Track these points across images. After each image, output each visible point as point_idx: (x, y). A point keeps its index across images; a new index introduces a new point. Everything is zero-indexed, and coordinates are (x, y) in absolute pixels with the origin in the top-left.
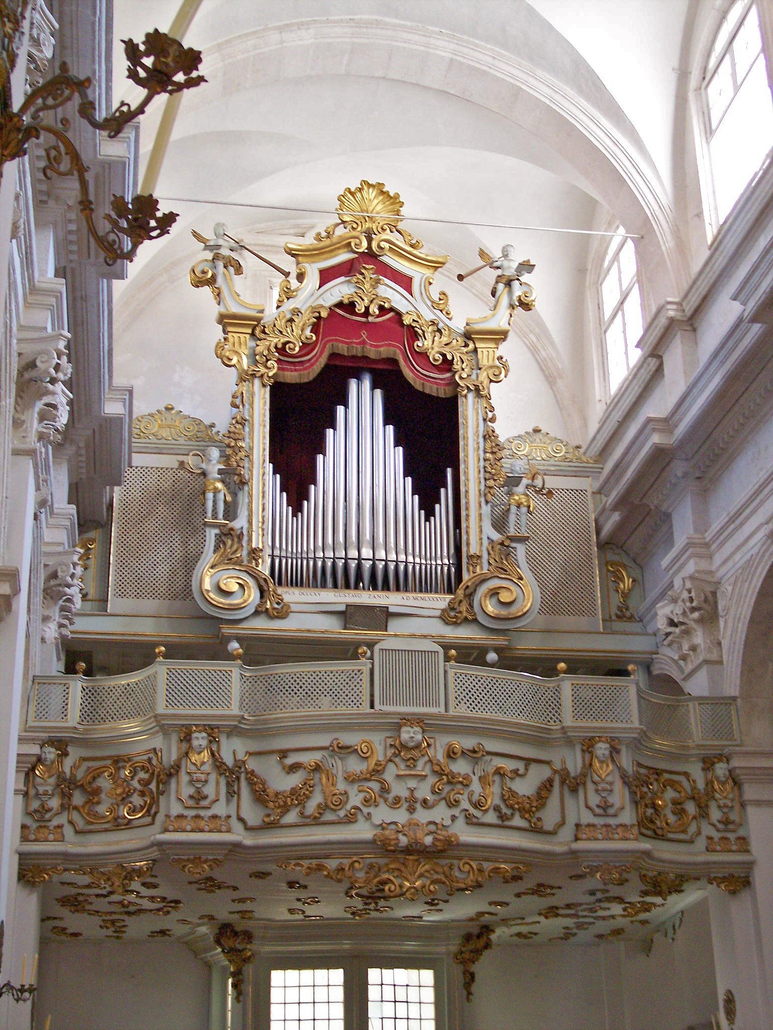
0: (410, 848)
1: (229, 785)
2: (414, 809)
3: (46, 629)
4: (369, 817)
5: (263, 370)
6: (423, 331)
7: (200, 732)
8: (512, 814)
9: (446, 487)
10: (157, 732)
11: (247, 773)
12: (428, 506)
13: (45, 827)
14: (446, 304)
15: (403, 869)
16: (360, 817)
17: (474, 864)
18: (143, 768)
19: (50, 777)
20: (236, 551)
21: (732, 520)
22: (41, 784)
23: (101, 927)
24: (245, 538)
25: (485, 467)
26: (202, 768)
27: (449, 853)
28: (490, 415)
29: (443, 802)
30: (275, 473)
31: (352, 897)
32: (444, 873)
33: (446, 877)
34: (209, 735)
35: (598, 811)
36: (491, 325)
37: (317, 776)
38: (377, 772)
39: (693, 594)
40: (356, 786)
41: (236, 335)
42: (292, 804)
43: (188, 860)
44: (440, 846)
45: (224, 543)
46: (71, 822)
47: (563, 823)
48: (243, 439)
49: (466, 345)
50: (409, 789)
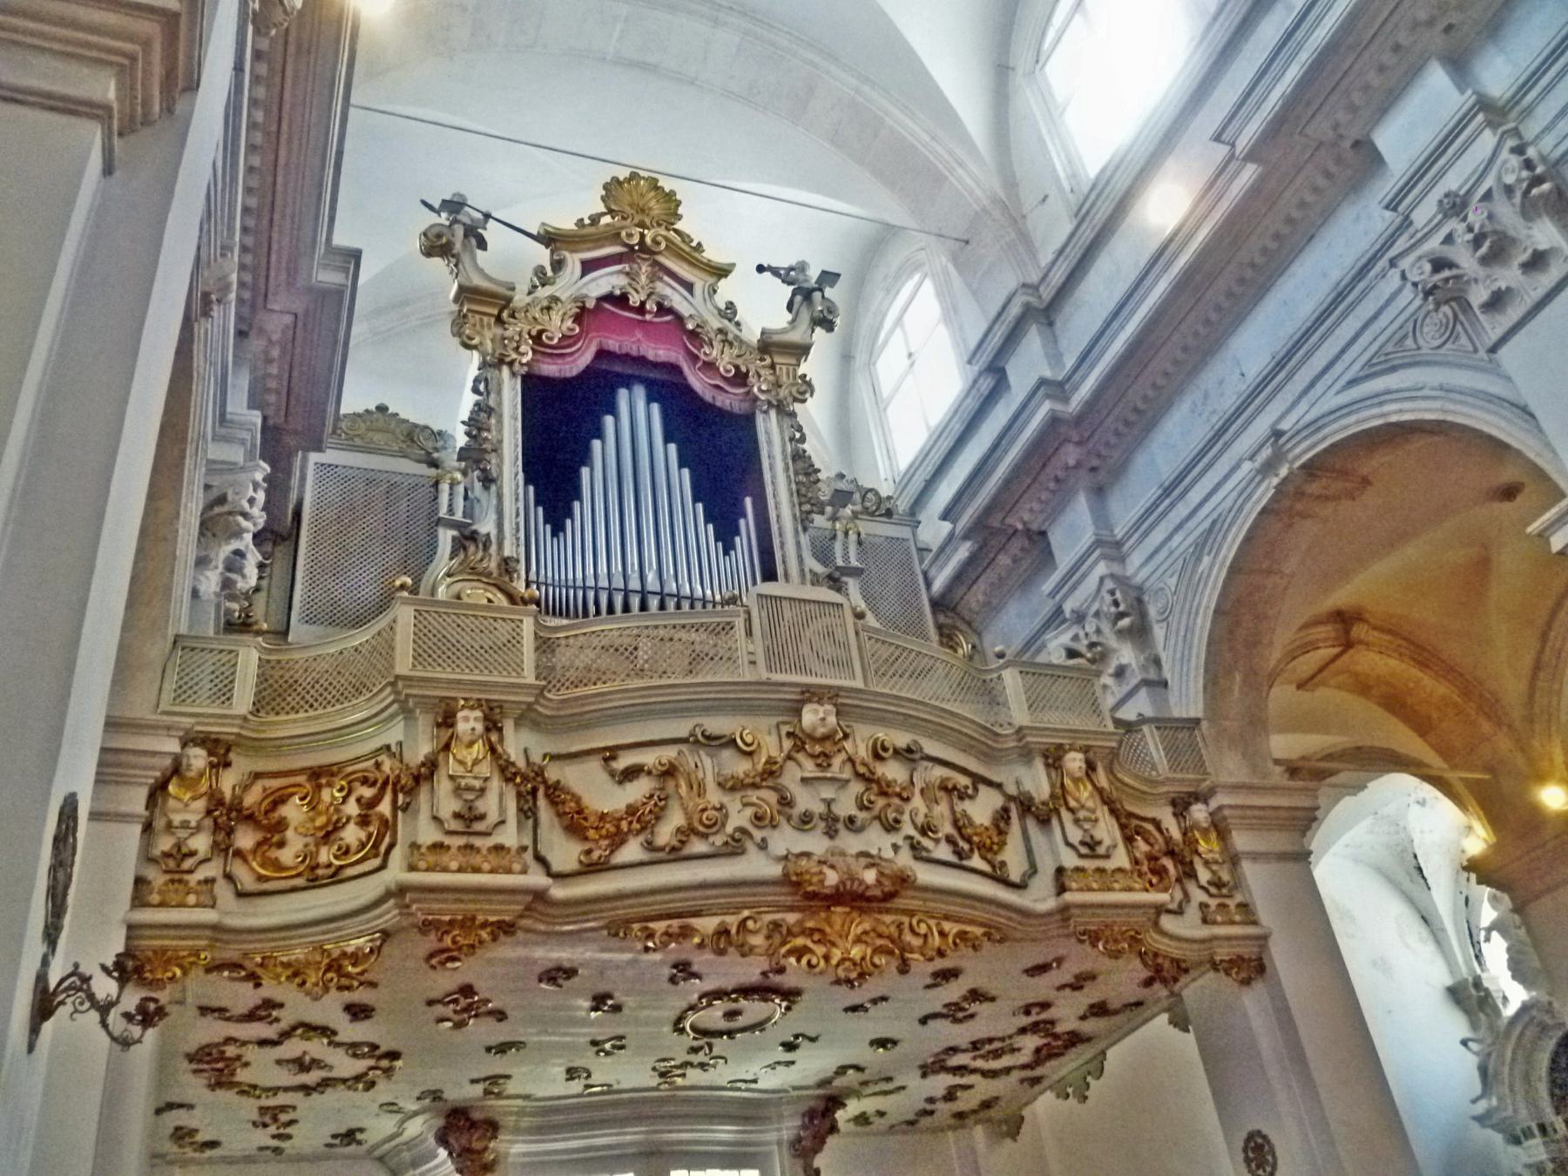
0: (841, 888)
1: (519, 795)
2: (836, 831)
3: (202, 578)
4: (763, 846)
5: (514, 356)
6: (711, 340)
7: (472, 708)
8: (972, 850)
9: (744, 515)
10: (392, 717)
11: (548, 787)
12: (726, 536)
13: (180, 881)
14: (735, 313)
15: (828, 930)
16: (749, 845)
17: (932, 922)
18: (365, 781)
19: (194, 798)
20: (482, 560)
21: (1167, 491)
22: (176, 811)
23: (255, 1124)
24: (493, 549)
25: (798, 491)
26: (476, 769)
27: (899, 903)
28: (798, 435)
29: (876, 824)
30: (527, 483)
31: (682, 1031)
32: (889, 937)
33: (893, 941)
34: (486, 718)
35: (1084, 850)
36: (796, 337)
37: (671, 784)
38: (771, 772)
39: (1118, 595)
40: (738, 796)
41: (478, 317)
42: (630, 831)
43: (451, 923)
44: (888, 886)
45: (465, 549)
46: (229, 877)
47: (1033, 870)
48: (488, 430)
49: (762, 360)
50: (824, 800)
